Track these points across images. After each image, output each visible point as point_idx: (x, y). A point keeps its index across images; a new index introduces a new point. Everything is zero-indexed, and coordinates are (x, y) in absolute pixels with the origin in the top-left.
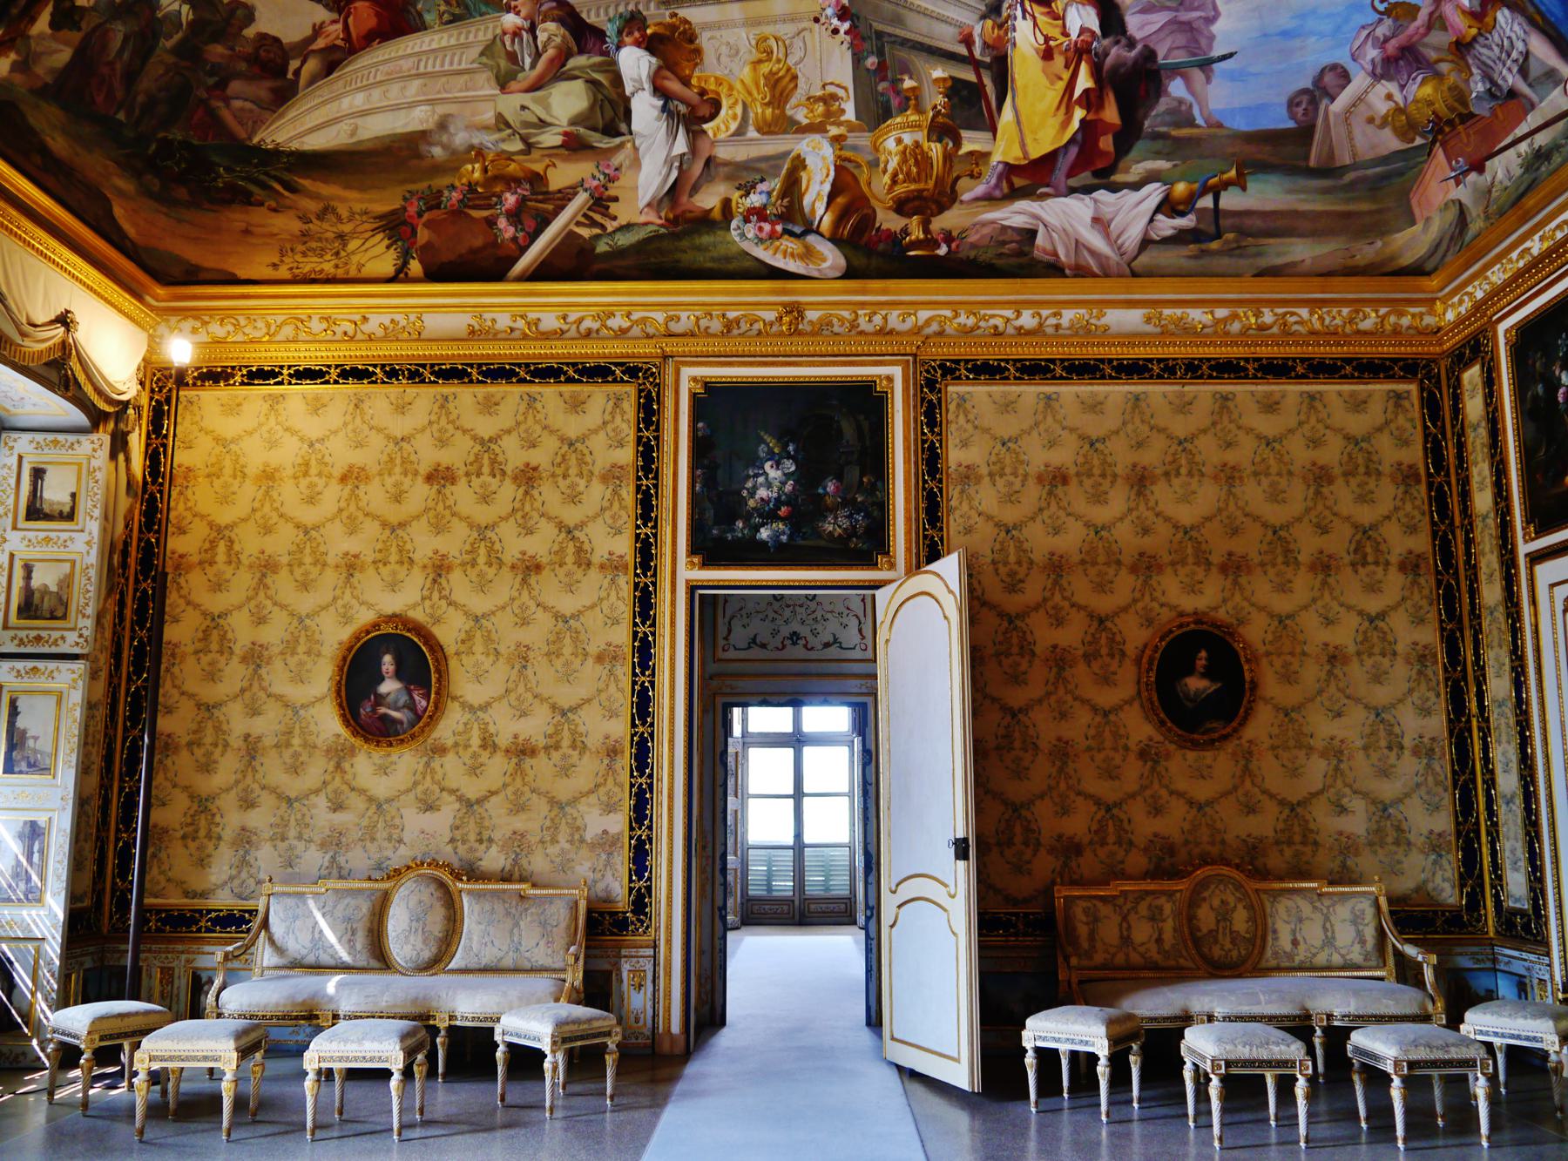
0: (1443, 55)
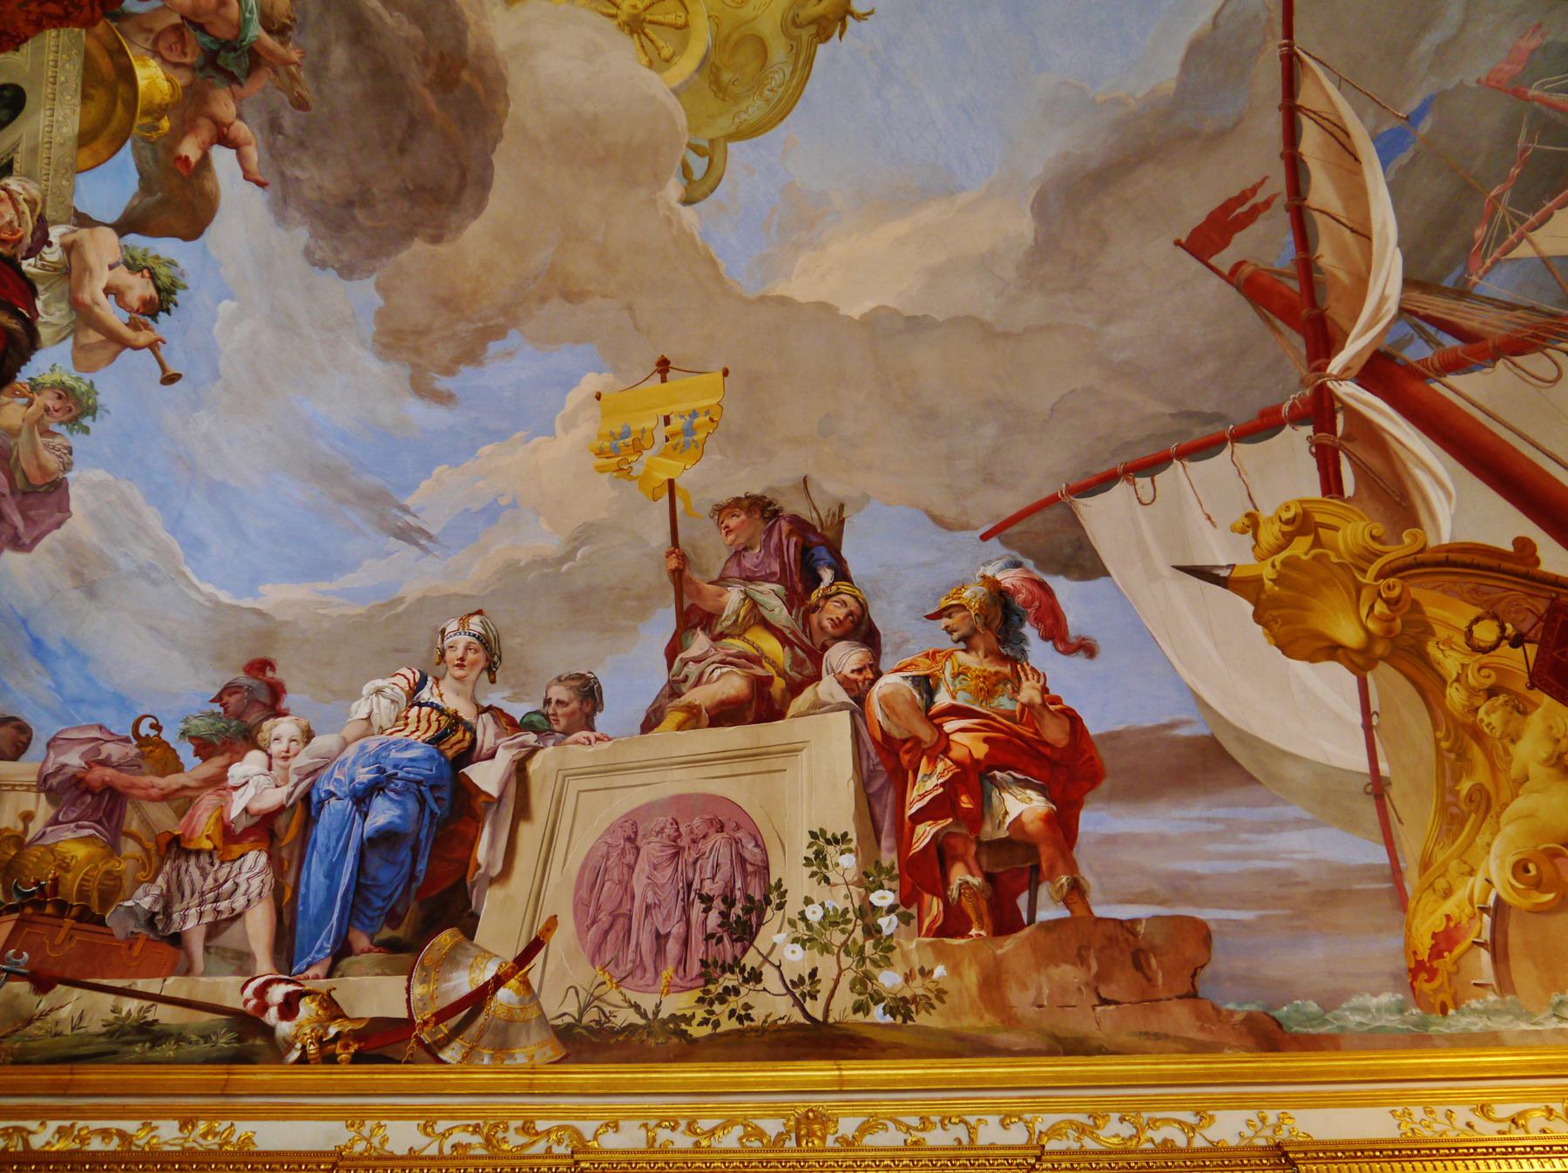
0: (143, 835)
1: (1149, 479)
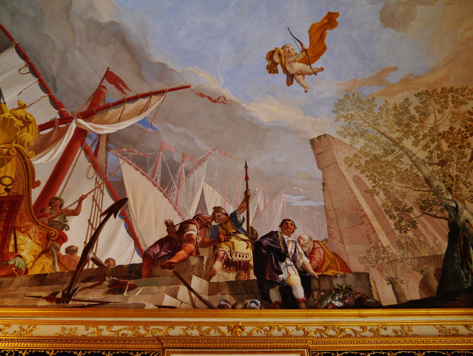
1: (28, 71)
